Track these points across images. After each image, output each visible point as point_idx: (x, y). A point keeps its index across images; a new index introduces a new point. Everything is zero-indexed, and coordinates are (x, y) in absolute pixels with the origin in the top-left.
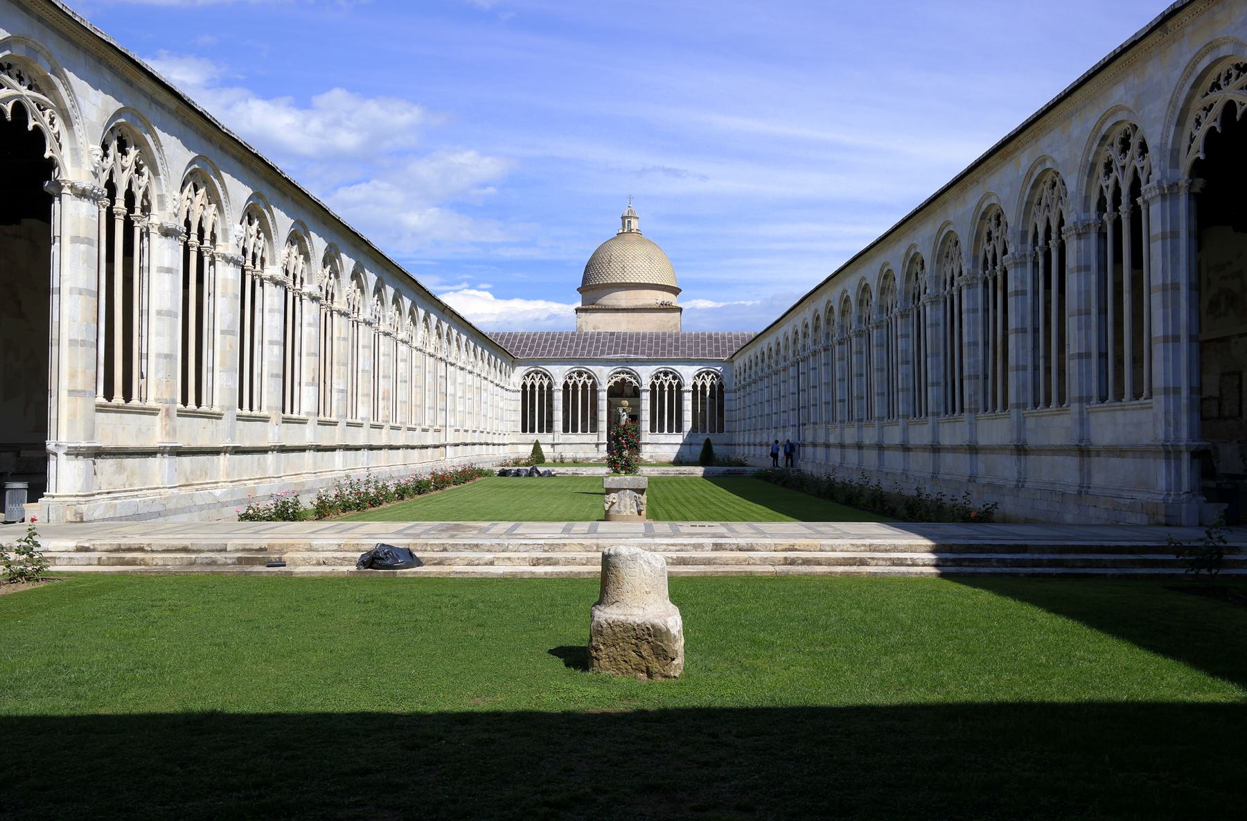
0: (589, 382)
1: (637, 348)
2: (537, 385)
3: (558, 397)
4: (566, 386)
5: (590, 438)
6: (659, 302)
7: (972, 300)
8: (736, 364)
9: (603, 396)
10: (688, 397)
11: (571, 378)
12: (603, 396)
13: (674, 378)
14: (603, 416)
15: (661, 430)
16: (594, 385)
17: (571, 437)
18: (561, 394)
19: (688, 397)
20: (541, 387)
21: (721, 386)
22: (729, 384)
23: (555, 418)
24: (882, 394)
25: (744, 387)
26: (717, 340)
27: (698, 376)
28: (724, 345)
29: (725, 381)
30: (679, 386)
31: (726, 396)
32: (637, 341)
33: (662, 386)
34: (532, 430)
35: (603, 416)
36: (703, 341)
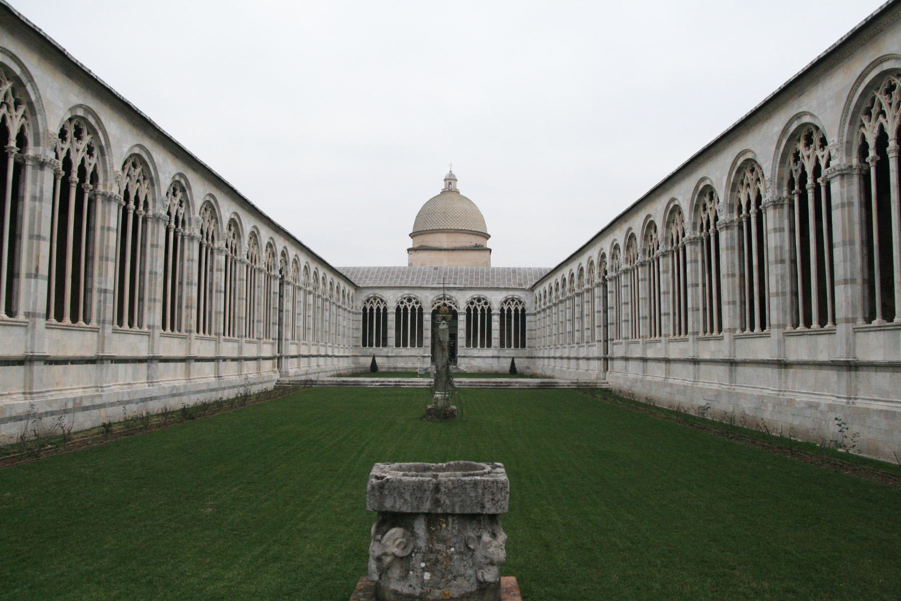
0: (417, 307)
1: (455, 279)
2: (375, 308)
3: (391, 318)
4: (398, 309)
5: (416, 351)
6: (473, 244)
7: (694, 253)
8: (537, 292)
9: (427, 317)
10: (496, 320)
11: (402, 303)
12: (427, 317)
13: (486, 303)
14: (427, 334)
15: (475, 346)
16: (421, 309)
17: (403, 351)
18: (394, 316)
19: (496, 320)
20: (378, 309)
21: (523, 310)
22: (530, 308)
23: (389, 335)
24: (734, 303)
25: (544, 310)
26: (520, 274)
27: (505, 302)
28: (525, 277)
29: (527, 306)
30: (489, 310)
31: (528, 318)
32: (456, 274)
33: (475, 310)
34: (371, 345)
35: (427, 334)
36: (509, 274)
